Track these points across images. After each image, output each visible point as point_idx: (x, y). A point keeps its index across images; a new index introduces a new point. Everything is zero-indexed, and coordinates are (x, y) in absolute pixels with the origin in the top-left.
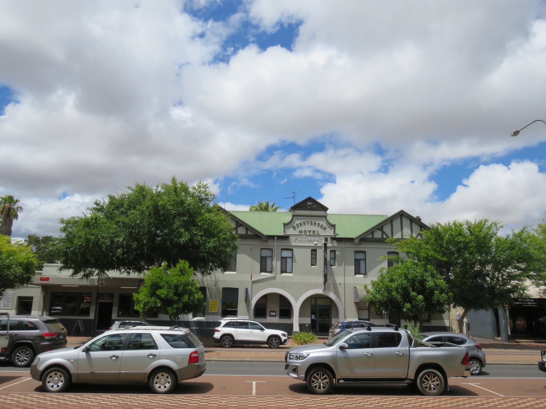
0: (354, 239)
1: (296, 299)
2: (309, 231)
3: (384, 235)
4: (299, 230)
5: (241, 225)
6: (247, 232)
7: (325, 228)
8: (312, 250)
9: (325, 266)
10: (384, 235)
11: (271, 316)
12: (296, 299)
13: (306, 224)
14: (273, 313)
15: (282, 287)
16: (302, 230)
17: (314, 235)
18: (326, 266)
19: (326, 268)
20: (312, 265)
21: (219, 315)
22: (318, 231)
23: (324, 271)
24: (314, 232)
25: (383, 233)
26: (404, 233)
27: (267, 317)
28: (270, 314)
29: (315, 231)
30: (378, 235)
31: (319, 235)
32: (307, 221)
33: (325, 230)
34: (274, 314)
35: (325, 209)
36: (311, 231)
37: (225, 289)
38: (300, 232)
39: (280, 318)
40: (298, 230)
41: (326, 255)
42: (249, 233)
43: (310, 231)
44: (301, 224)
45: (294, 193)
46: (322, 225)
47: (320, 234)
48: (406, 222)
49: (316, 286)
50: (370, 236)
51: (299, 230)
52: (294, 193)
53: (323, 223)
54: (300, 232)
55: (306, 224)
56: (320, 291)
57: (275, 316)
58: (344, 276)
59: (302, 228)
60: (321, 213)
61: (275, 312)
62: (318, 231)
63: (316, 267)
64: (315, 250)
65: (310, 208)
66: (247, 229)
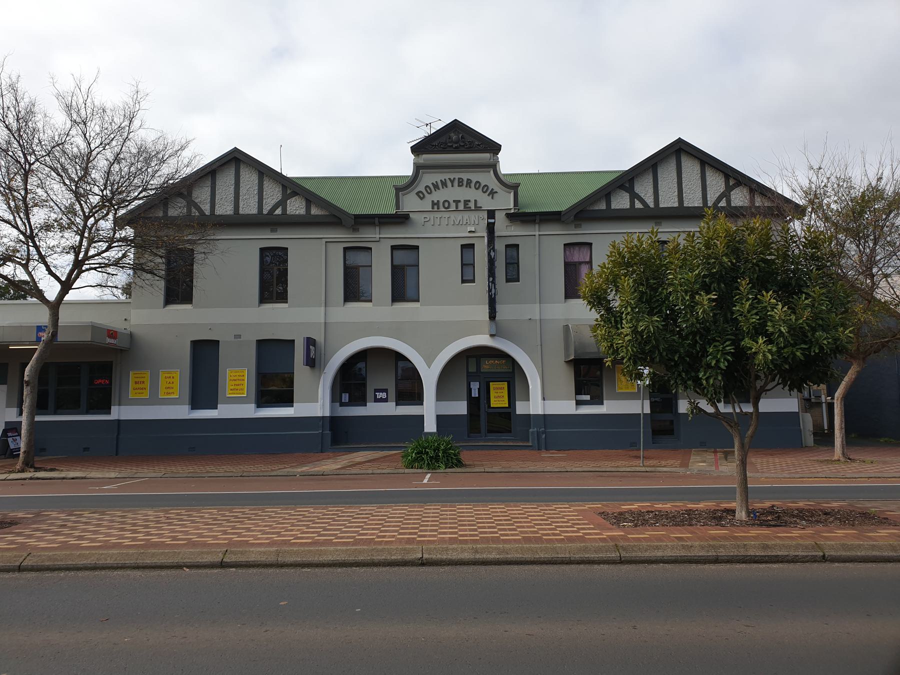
0: (562, 213)
1: (429, 363)
2: (454, 201)
3: (637, 202)
4: (433, 201)
5: (295, 194)
6: (308, 209)
7: (492, 193)
8: (463, 247)
9: (491, 279)
10: (637, 202)
11: (377, 400)
12: (429, 363)
13: (449, 184)
14: (381, 394)
15: (396, 331)
16: (438, 201)
17: (467, 208)
18: (494, 279)
19: (493, 282)
20: (463, 281)
21: (332, 409)
22: (476, 201)
23: (490, 290)
24: (466, 202)
25: (634, 196)
26: (684, 195)
27: (368, 404)
28: (376, 396)
29: (469, 201)
30: (621, 202)
31: (478, 208)
32: (450, 179)
33: (492, 198)
34: (383, 395)
35: (495, 148)
36: (459, 201)
37: (261, 343)
38: (435, 204)
39: (397, 405)
40: (429, 199)
41: (492, 254)
42: (314, 211)
43: (457, 202)
44: (436, 186)
45: (429, 127)
46: (486, 186)
47: (481, 207)
48: (691, 169)
49: (470, 329)
50: (603, 206)
51: (433, 201)
52: (429, 127)
53: (487, 178)
54: (435, 204)
55: (449, 184)
56: (483, 340)
57: (385, 400)
58: (540, 303)
59: (439, 196)
60: (486, 156)
61: (386, 391)
62: (476, 201)
63: (474, 284)
64: (472, 246)
65: (456, 148)
66: (309, 203)
